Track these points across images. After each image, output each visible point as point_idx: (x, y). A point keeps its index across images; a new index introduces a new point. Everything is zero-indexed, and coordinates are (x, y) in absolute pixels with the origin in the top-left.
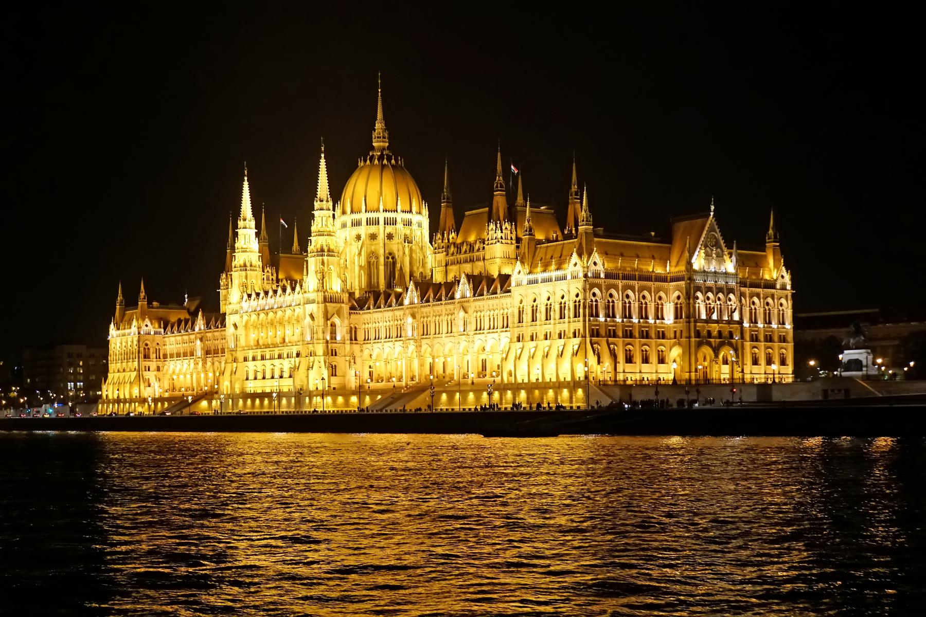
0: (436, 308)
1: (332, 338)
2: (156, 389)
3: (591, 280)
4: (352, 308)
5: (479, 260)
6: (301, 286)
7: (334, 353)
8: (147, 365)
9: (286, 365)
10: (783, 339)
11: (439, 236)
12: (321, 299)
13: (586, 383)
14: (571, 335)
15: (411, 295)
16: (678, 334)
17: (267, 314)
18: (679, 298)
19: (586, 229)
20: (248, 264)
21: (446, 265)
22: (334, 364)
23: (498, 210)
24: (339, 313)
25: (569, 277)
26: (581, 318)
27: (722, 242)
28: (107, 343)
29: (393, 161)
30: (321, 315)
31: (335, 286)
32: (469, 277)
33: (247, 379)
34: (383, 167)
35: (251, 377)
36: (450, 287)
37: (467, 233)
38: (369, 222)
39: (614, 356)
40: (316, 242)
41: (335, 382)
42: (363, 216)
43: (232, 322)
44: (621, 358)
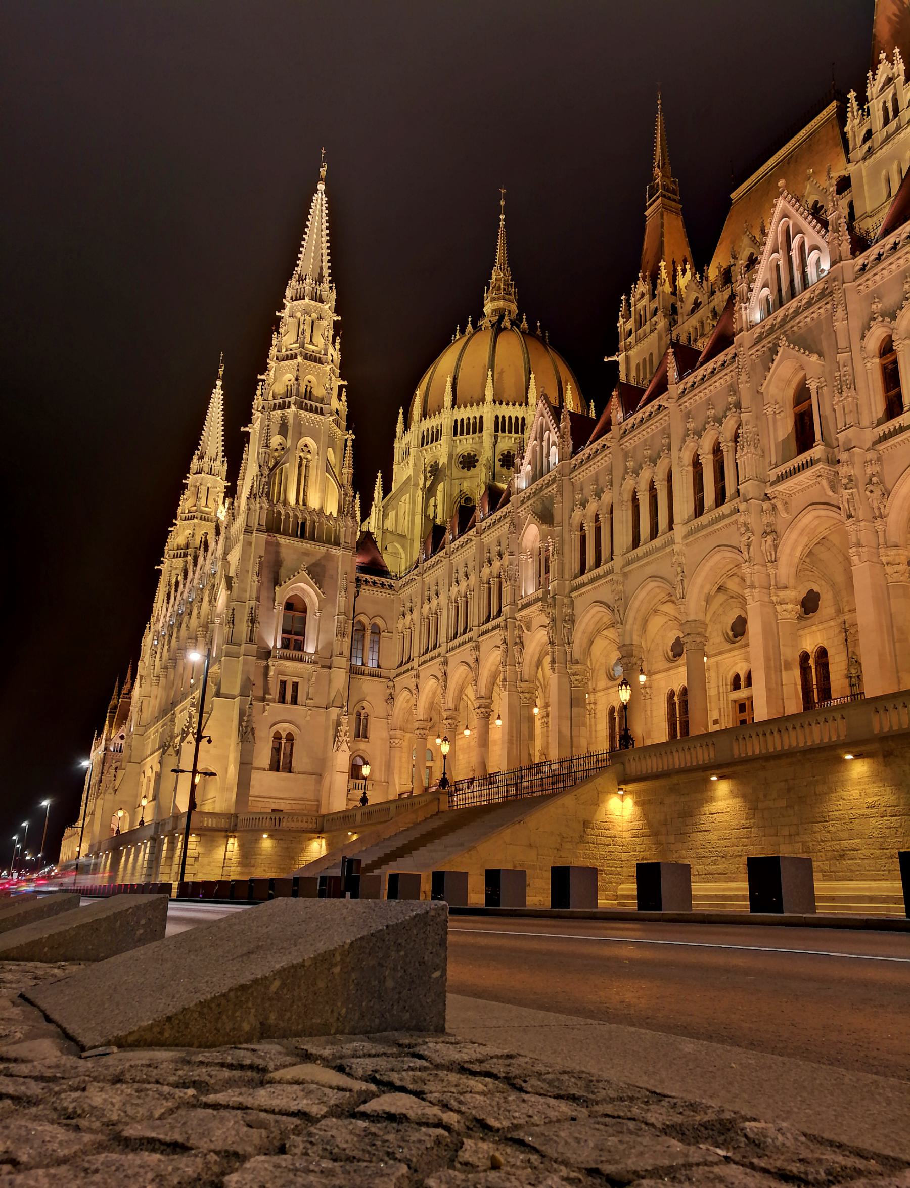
1: (286, 645)
7: (289, 694)
22: (284, 728)
24: (318, 573)
38: (459, 428)
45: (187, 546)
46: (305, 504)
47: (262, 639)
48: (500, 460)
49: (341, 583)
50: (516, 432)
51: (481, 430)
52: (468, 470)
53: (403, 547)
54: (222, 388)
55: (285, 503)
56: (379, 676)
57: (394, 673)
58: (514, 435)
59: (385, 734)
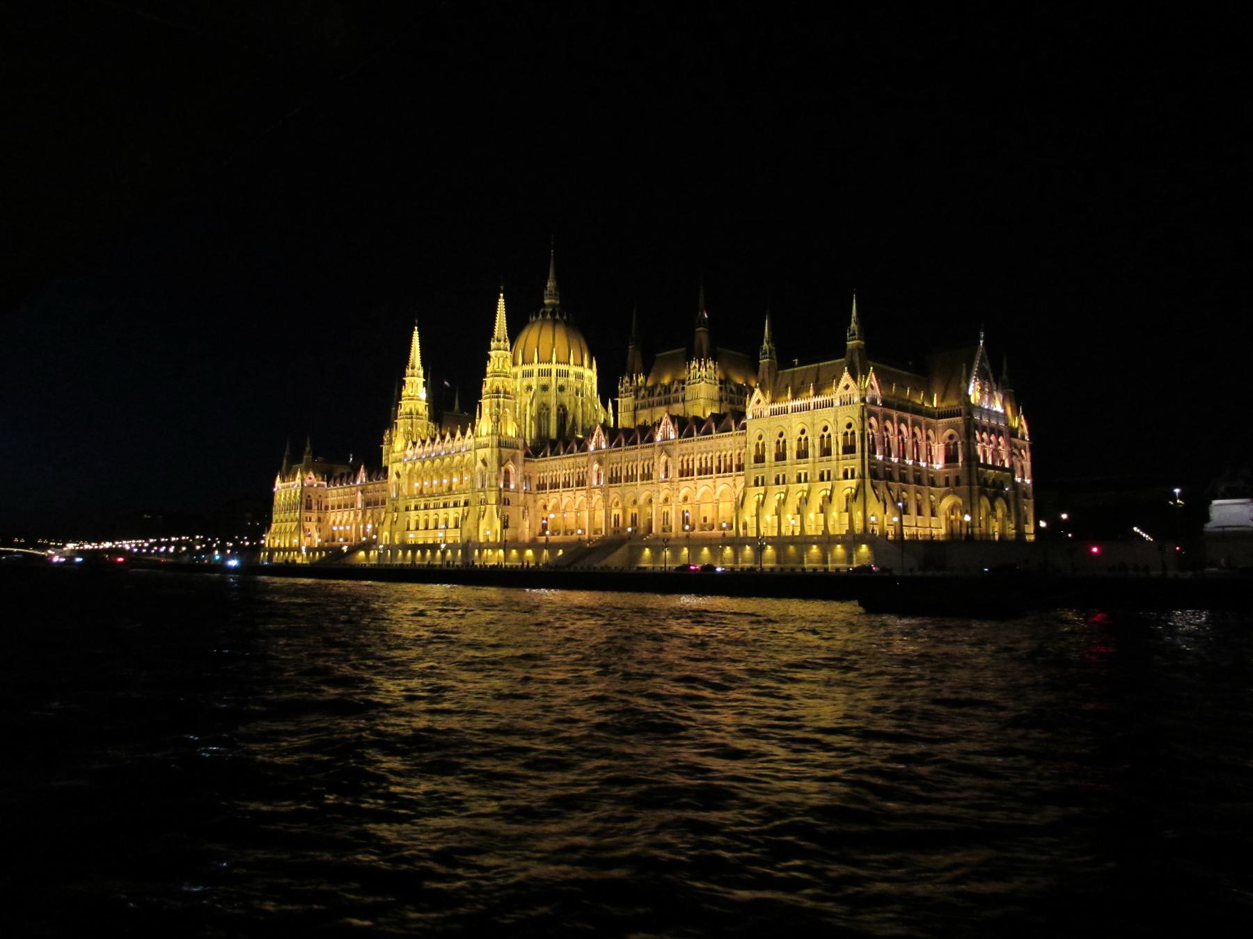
2: (317, 541)
4: (527, 455)
5: (676, 401)
7: (506, 502)
8: (307, 517)
9: (453, 513)
10: (1025, 496)
11: (627, 379)
12: (495, 443)
13: (866, 536)
14: (841, 476)
15: (598, 440)
16: (952, 481)
17: (433, 462)
18: (951, 437)
21: (636, 409)
23: (701, 345)
24: (514, 459)
25: (837, 403)
26: (858, 454)
27: (991, 375)
28: (273, 494)
30: (495, 458)
31: (511, 431)
33: (408, 529)
35: (412, 527)
37: (660, 375)
40: (489, 383)
41: (509, 533)
42: (535, 367)
45: (411, 413)
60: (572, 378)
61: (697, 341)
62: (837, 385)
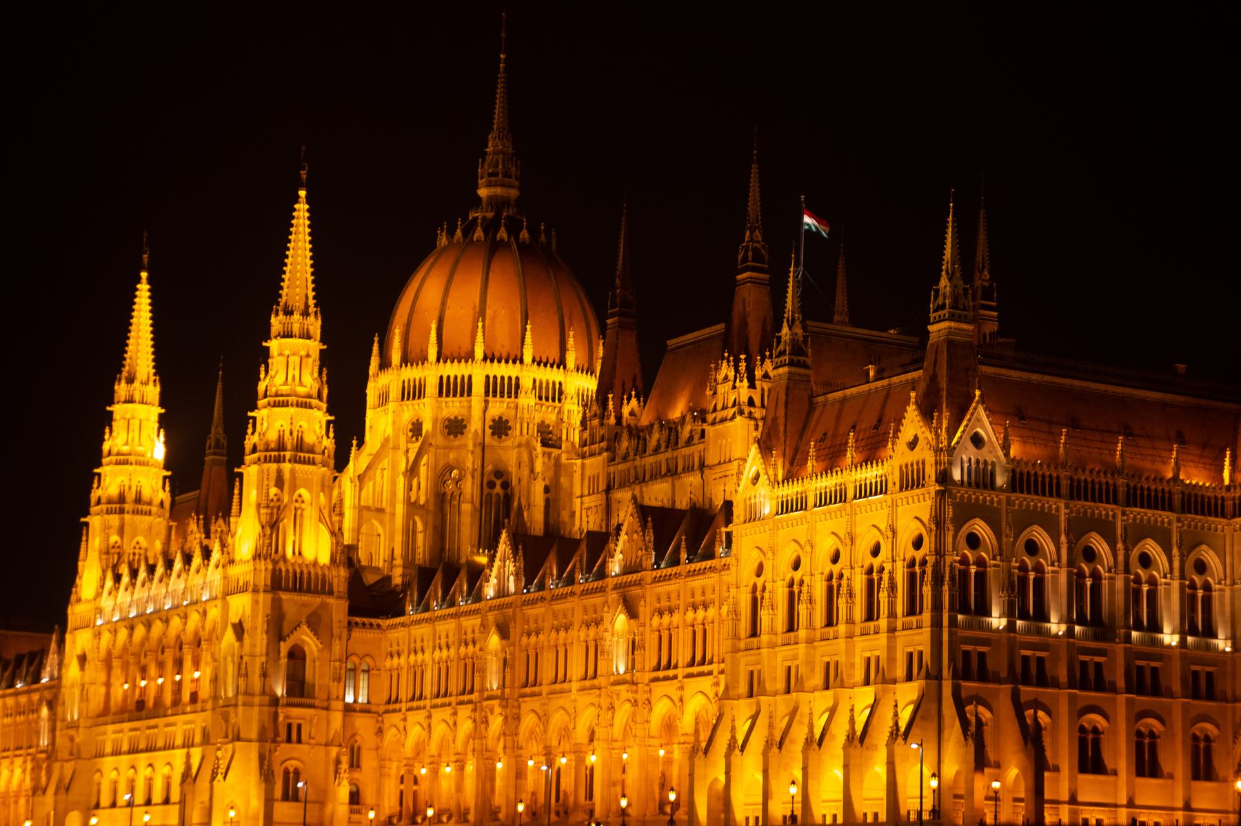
0: (559, 607)
1: (290, 692)
3: (961, 493)
5: (688, 469)
6: (223, 545)
7: (293, 735)
12: (263, 579)
15: (502, 572)
19: (950, 331)
20: (131, 496)
21: (608, 489)
22: (292, 765)
23: (744, 324)
24: (315, 622)
26: (926, 616)
29: (524, 235)
31: (314, 546)
32: (644, 512)
33: (97, 806)
34: (494, 248)
35: (105, 800)
36: (599, 542)
37: (668, 399)
38: (448, 388)
39: (1033, 739)
43: (79, 652)
44: (1062, 751)
45: (122, 499)
46: (300, 554)
47: (272, 689)
48: (490, 427)
49: (336, 631)
50: (509, 397)
51: (470, 394)
52: (456, 436)
53: (381, 522)
54: (149, 281)
55: (284, 557)
56: (368, 712)
57: (382, 709)
58: (506, 399)
59: (375, 764)
60: (527, 400)
61: (737, 308)
62: (896, 437)
